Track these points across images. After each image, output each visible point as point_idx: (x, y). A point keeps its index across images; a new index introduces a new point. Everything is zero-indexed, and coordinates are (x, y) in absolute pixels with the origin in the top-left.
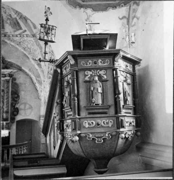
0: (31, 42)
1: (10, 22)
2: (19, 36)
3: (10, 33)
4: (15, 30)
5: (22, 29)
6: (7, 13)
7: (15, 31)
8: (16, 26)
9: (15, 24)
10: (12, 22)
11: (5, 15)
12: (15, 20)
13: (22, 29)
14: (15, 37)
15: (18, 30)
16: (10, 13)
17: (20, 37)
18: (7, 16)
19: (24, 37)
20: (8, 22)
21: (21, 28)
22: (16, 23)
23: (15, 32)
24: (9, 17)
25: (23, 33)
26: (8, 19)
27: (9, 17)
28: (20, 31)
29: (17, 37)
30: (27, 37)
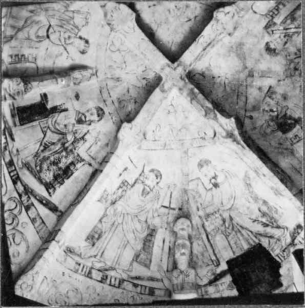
0: (23, 245)
1: (53, 144)
2: (21, 188)
3: (15, 152)
4: (33, 165)
5: (51, 196)
6: (83, 128)
7: (27, 166)
11: (74, 121)
14: (10, 173)
15: (40, 180)
17: (20, 196)
19: (27, 208)
20: (51, 137)
23: (27, 172)
25: (41, 201)
27: (70, 138)
28: (41, 190)
29: (15, 183)
30: (33, 221)
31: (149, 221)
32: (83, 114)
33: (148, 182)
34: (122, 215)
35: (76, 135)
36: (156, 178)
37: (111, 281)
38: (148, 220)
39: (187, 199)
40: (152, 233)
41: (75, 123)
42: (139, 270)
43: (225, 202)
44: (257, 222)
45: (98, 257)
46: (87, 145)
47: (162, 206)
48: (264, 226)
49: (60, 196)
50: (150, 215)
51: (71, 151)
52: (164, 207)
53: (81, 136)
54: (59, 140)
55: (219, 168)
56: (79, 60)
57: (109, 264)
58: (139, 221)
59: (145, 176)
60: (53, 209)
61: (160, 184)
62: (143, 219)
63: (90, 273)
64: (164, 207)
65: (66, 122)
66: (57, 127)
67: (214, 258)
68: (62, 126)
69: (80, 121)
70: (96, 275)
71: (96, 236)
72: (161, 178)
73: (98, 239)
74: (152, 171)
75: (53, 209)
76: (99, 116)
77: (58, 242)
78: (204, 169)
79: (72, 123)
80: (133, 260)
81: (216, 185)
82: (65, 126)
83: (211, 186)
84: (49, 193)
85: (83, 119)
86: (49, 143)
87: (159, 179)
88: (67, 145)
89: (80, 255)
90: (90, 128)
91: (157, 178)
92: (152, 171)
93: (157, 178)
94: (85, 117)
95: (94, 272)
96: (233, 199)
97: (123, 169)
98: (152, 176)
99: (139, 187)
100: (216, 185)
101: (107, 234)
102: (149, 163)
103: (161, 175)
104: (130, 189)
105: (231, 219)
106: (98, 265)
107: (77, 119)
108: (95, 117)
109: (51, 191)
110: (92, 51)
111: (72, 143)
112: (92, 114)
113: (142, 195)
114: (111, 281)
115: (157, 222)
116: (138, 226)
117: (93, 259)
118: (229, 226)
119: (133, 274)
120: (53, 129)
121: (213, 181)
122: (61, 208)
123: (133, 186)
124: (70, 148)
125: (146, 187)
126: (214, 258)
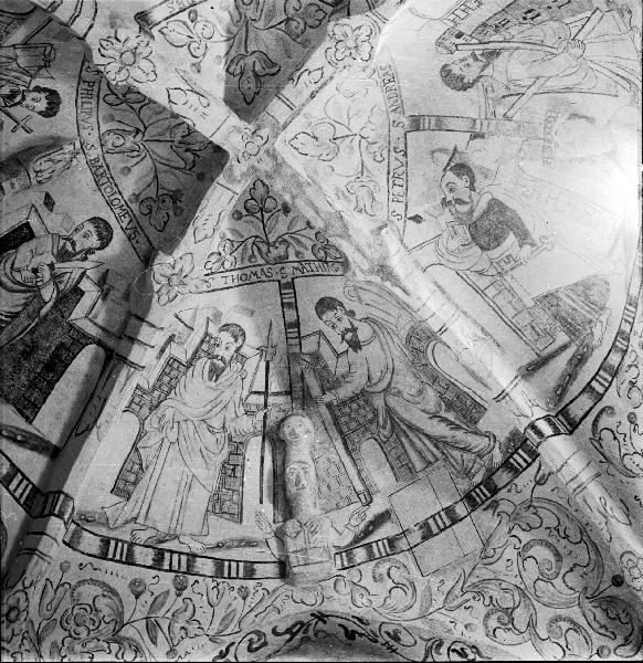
1: (18, 314)
5: (31, 423)
6: (72, 269)
8: (17, 368)
9: (27, 354)
10: (23, 321)
11: (50, 259)
12: (59, 337)
13: (29, 421)
16: (85, 285)
18: (47, 274)
21: (29, 408)
22: (44, 356)
24: (48, 293)
25: (14, 440)
26: (34, 290)
27: (48, 293)
31: (231, 426)
32: (68, 239)
33: (219, 351)
34: (176, 425)
35: (62, 287)
36: (233, 340)
37: (171, 564)
38: (227, 426)
39: (300, 373)
40: (237, 447)
41: (55, 261)
42: (222, 530)
43: (376, 375)
44: (437, 419)
45: (141, 520)
46: (86, 301)
47: (252, 393)
48: (451, 429)
49: (50, 421)
50: (230, 414)
51: (55, 321)
52: (256, 393)
53: (72, 283)
54: (26, 305)
55: (360, 312)
56: (42, 128)
57: (163, 527)
58: (210, 429)
59: (212, 342)
60: (37, 444)
61: (243, 351)
62: (217, 423)
63: (130, 553)
64: (256, 393)
65: (34, 265)
66: (18, 278)
67: (360, 487)
68: (28, 274)
69: (64, 256)
70: (144, 556)
71: (132, 478)
72: (244, 341)
73: (135, 484)
74: (226, 327)
75: (37, 444)
76: (101, 238)
77: (60, 516)
78: (329, 315)
79: (49, 262)
80: (208, 511)
81: (356, 345)
82: (35, 271)
83: (345, 346)
84: (27, 418)
85: (69, 247)
86: (6, 316)
87: (240, 341)
88: (44, 311)
89: (106, 524)
90: (87, 264)
91: (236, 341)
92: (226, 327)
93: (236, 341)
94: (73, 244)
95: (137, 550)
96: (389, 376)
97: (164, 340)
98: (226, 337)
99: (203, 364)
100: (356, 345)
101: (151, 469)
102: (218, 315)
103: (244, 334)
104: (185, 374)
105: (389, 411)
106: (143, 536)
107: (55, 251)
108: (94, 241)
109: (28, 413)
110: (67, 109)
111: (55, 306)
112: (85, 236)
113: (210, 379)
114: (171, 564)
115: (246, 424)
116: (209, 439)
117: (132, 526)
118: (385, 421)
119: (212, 540)
120: (10, 284)
121: (349, 336)
122: (54, 438)
123: (190, 364)
124: (51, 317)
125: (215, 360)
126: (360, 487)
